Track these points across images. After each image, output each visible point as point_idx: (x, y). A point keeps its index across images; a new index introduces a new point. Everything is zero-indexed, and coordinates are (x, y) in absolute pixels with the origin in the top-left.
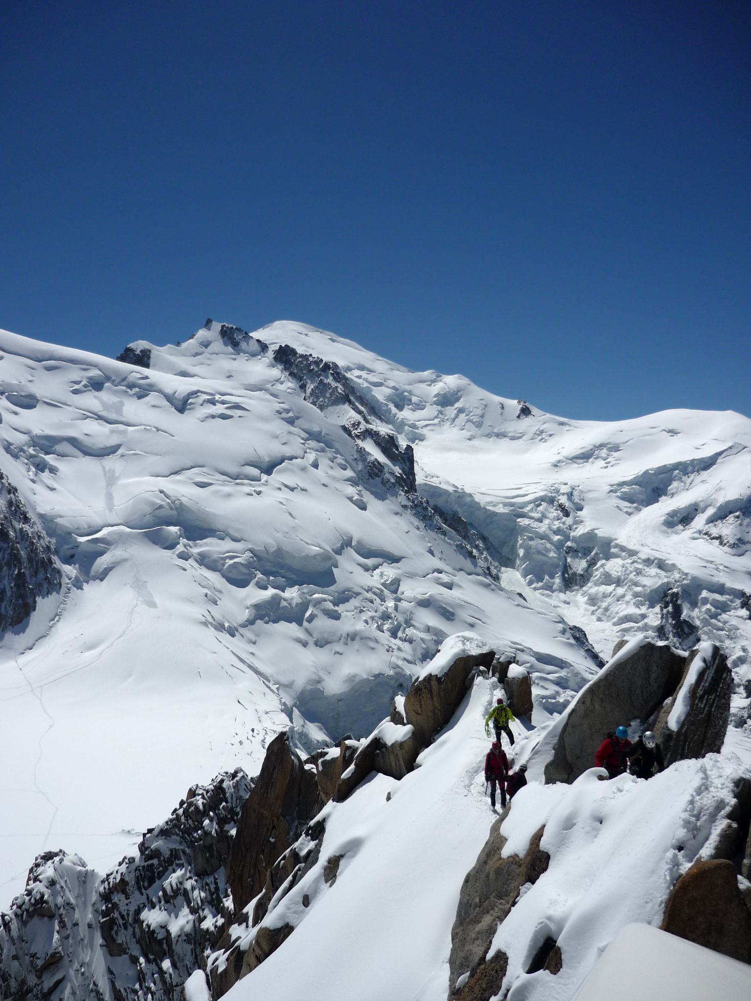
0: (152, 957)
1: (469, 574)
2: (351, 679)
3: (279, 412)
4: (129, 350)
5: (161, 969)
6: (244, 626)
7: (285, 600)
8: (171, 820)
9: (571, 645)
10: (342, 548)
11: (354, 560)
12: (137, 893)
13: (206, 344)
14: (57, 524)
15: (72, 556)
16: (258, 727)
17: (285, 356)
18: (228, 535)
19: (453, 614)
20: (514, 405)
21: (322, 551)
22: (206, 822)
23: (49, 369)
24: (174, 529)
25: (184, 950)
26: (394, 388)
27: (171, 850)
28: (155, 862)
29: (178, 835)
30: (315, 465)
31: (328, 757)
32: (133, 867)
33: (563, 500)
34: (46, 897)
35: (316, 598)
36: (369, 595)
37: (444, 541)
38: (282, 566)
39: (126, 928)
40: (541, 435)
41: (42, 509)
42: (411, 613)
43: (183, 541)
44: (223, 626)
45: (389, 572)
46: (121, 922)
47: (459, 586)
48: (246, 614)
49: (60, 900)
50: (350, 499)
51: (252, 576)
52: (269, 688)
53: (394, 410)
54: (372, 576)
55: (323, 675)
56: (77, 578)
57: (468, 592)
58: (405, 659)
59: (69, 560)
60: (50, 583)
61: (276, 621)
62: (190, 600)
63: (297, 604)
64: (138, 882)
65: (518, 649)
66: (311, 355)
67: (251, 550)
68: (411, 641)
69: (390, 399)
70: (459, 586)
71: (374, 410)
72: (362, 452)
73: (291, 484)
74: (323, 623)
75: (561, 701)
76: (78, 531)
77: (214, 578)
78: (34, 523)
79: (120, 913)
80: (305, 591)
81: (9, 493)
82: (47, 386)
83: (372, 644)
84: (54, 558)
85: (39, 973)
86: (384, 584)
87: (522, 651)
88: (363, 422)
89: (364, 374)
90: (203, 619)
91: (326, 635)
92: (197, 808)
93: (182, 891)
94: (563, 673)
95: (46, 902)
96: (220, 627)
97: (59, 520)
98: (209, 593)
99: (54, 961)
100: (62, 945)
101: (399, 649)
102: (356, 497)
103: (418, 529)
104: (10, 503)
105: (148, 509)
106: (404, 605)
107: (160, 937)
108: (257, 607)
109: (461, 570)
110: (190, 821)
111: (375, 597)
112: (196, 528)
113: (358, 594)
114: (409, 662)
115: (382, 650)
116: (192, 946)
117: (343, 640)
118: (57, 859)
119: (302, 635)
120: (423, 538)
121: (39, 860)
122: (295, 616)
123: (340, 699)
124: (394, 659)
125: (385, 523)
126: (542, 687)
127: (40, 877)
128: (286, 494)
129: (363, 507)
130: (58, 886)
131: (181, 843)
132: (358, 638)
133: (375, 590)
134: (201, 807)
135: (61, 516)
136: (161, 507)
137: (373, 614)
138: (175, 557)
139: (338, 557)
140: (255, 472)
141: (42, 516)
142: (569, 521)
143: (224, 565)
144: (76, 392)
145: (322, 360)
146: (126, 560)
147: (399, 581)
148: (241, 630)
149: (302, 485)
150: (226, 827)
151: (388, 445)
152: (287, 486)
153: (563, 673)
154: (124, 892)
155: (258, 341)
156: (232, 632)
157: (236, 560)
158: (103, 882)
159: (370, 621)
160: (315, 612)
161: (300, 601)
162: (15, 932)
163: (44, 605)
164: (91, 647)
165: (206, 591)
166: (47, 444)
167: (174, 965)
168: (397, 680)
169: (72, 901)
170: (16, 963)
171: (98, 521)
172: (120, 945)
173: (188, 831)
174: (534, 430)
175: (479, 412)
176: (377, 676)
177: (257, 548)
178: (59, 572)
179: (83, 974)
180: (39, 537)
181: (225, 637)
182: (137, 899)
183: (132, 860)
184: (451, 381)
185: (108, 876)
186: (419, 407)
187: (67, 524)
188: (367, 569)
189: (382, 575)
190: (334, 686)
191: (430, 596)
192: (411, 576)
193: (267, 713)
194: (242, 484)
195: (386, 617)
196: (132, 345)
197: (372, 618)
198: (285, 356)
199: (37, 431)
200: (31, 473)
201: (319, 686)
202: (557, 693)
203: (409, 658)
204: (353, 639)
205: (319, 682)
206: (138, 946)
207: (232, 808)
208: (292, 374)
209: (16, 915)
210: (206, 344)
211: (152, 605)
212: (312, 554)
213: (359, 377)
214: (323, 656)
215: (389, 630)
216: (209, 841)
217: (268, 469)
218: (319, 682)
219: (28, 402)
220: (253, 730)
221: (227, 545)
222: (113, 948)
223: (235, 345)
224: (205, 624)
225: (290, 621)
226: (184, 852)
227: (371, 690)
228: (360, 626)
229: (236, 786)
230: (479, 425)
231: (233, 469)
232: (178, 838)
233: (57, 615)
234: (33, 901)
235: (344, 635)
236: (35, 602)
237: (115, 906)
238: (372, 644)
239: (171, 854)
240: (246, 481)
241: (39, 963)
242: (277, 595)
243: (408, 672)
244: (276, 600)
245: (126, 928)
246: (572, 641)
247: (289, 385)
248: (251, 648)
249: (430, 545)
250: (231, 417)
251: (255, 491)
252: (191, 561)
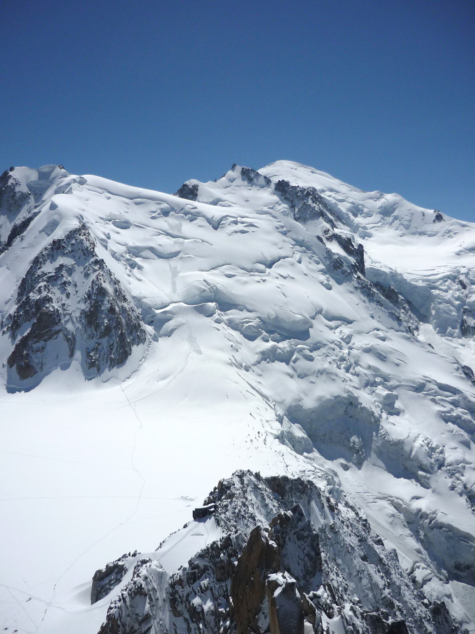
0: (194, 620)
1: (397, 331)
2: (320, 399)
3: (277, 228)
4: (185, 186)
5: (199, 627)
6: (255, 365)
7: (280, 349)
8: (205, 550)
9: (462, 378)
10: (316, 315)
11: (323, 323)
12: (187, 586)
13: (232, 180)
14: (143, 302)
15: (152, 322)
16: (262, 431)
17: (283, 188)
18: (245, 308)
19: (385, 357)
21: (303, 318)
22: (222, 555)
23: (137, 204)
24: (212, 305)
25: (210, 619)
26: (352, 203)
27: (205, 566)
28: (197, 571)
29: (208, 558)
30: (300, 262)
31: (270, 579)
32: (186, 572)
33: (462, 278)
34: (143, 586)
35: (300, 348)
36: (332, 346)
37: (381, 309)
38: (278, 327)
39: (182, 603)
40: (449, 234)
41: (135, 293)
42: (359, 357)
43: (218, 312)
44: (241, 366)
45: (346, 330)
46: (180, 600)
47: (390, 339)
48: (256, 358)
49: (150, 587)
50: (322, 283)
51: (260, 334)
52: (269, 405)
53: (352, 217)
54: (335, 333)
55: (302, 396)
56: (155, 336)
57: (396, 343)
58: (354, 387)
59: (150, 323)
60: (140, 339)
61: (273, 362)
62: (222, 349)
63: (287, 351)
64: (188, 580)
65: (427, 381)
66: (298, 186)
67: (259, 318)
68: (358, 375)
69: (350, 210)
70: (390, 339)
71: (340, 217)
72: (329, 252)
73: (285, 274)
74: (303, 364)
75: (454, 415)
76: (155, 307)
77: (236, 335)
78: (130, 302)
79: (179, 595)
80: (293, 343)
81: (115, 284)
82: (136, 215)
83: (334, 377)
84: (142, 323)
85: (140, 623)
86: (342, 339)
87: (430, 382)
88: (331, 229)
89: (333, 194)
90: (230, 361)
91: (305, 371)
92: (217, 546)
93: (210, 588)
94: (456, 397)
95: (143, 589)
96: (239, 366)
97: (144, 300)
98: (233, 344)
99: (147, 618)
100: (151, 610)
101: (351, 380)
102: (326, 282)
103: (364, 302)
104: (116, 291)
105: (197, 292)
106: (354, 352)
107: (199, 610)
108: (263, 353)
109: (392, 328)
110: (214, 552)
111: (336, 347)
112: (226, 304)
113: (325, 345)
114: (356, 388)
115: (339, 381)
116: (214, 617)
117: (315, 374)
118: (148, 564)
119: (290, 371)
120: (367, 308)
121: (139, 563)
122: (286, 358)
123: (313, 411)
124: (347, 387)
125: (343, 299)
126: (442, 405)
127: (140, 575)
128: (281, 281)
129: (329, 288)
130: (149, 580)
131: (209, 562)
132: (324, 373)
133: (336, 342)
134: (219, 546)
135: (145, 298)
136: (204, 291)
137: (334, 358)
138: (213, 322)
139: (313, 321)
140: (262, 267)
141: (134, 297)
142: (466, 292)
143: (243, 327)
144: (153, 218)
146: (183, 324)
147: (352, 336)
148: (253, 368)
149: (291, 275)
150: (232, 559)
151: (346, 244)
152: (282, 276)
153: (456, 397)
154: (181, 585)
155: (265, 177)
156: (247, 369)
157: (250, 324)
158: (171, 578)
159: (332, 362)
160: (299, 356)
161: (289, 349)
162: (128, 603)
163: (137, 350)
164: (164, 378)
165: (231, 343)
166: (135, 251)
167: (205, 625)
168: (349, 400)
169: (156, 587)
170: (129, 618)
171: (167, 300)
172: (179, 612)
173: (212, 557)
174: (444, 229)
175: (408, 218)
176: (336, 397)
177: (263, 316)
178: (144, 331)
179: (161, 625)
180: (133, 310)
181: (243, 372)
182: (188, 589)
183: (185, 569)
184: (390, 198)
185: (173, 575)
186: (369, 215)
187: (150, 303)
188: (331, 328)
189: (341, 332)
190: (309, 403)
191: (372, 346)
192: (359, 333)
193: (267, 421)
194: (254, 275)
195: (343, 359)
196: (187, 183)
197: (334, 360)
199: (131, 244)
200: (127, 270)
201: (300, 403)
202: (452, 410)
203: (357, 386)
204: (322, 374)
205: (300, 400)
206: (188, 613)
207: (235, 550)
208: (286, 199)
209: (129, 594)
210: (232, 180)
211: (200, 352)
212: (297, 320)
213: (330, 196)
214: (303, 384)
215: (345, 368)
216: (223, 564)
217: (270, 265)
218: (300, 400)
219: (125, 225)
220: (259, 433)
221: (245, 314)
222: (176, 613)
223: (250, 180)
224: (231, 364)
225: (282, 361)
226: (211, 567)
227: (332, 406)
228: (326, 366)
229: (237, 538)
230: (407, 227)
231: (249, 266)
232: (208, 560)
233: (143, 357)
234: (137, 587)
235: (317, 371)
236: (131, 350)
237: (177, 592)
238: (334, 377)
239: (205, 567)
240: (257, 273)
241: (140, 618)
242: (275, 345)
243: (356, 395)
244: (274, 350)
245: (182, 603)
246: (464, 376)
247: (284, 206)
248: (259, 379)
249: (372, 312)
250: (247, 232)
251: (262, 280)
252: (222, 324)
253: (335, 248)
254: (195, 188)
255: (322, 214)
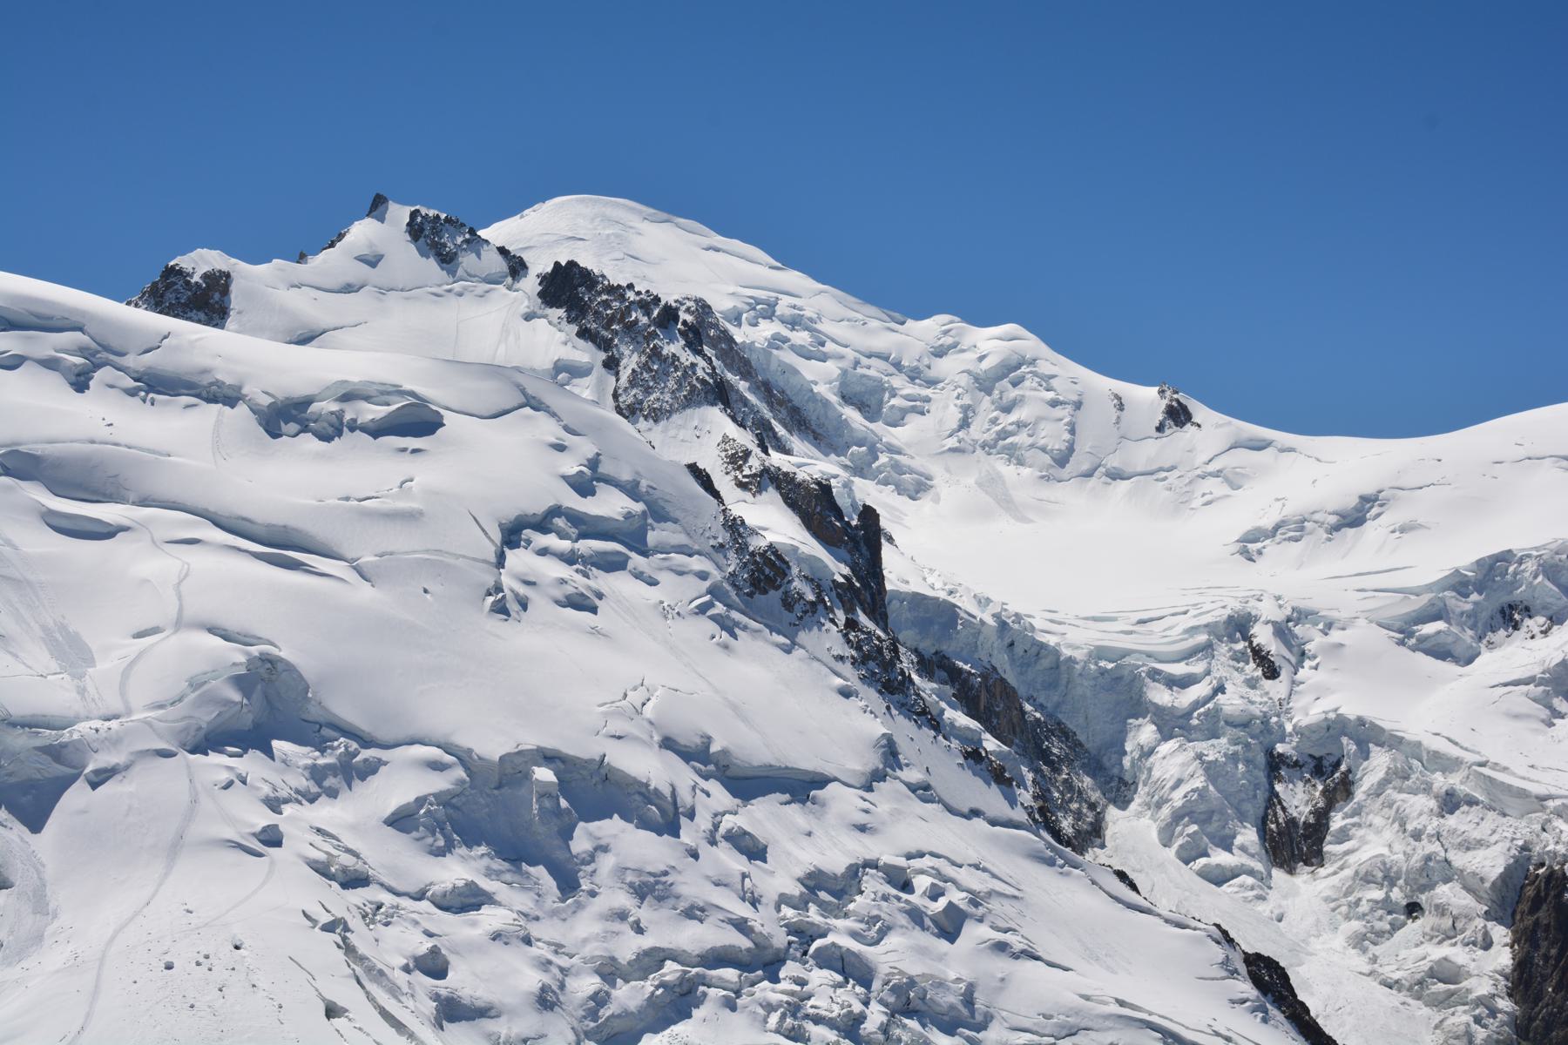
4: (172, 273)
17: (567, 288)
20: (1147, 399)
33: (1263, 635)
66: (631, 286)
72: (735, 527)
88: (757, 451)
142: (1277, 688)
145: (657, 300)
155: (503, 251)
184: (991, 342)
196: (183, 262)
198: (567, 288)
208: (584, 334)
223: (447, 260)
253: (775, 524)
254: (219, 283)
255: (720, 394)
